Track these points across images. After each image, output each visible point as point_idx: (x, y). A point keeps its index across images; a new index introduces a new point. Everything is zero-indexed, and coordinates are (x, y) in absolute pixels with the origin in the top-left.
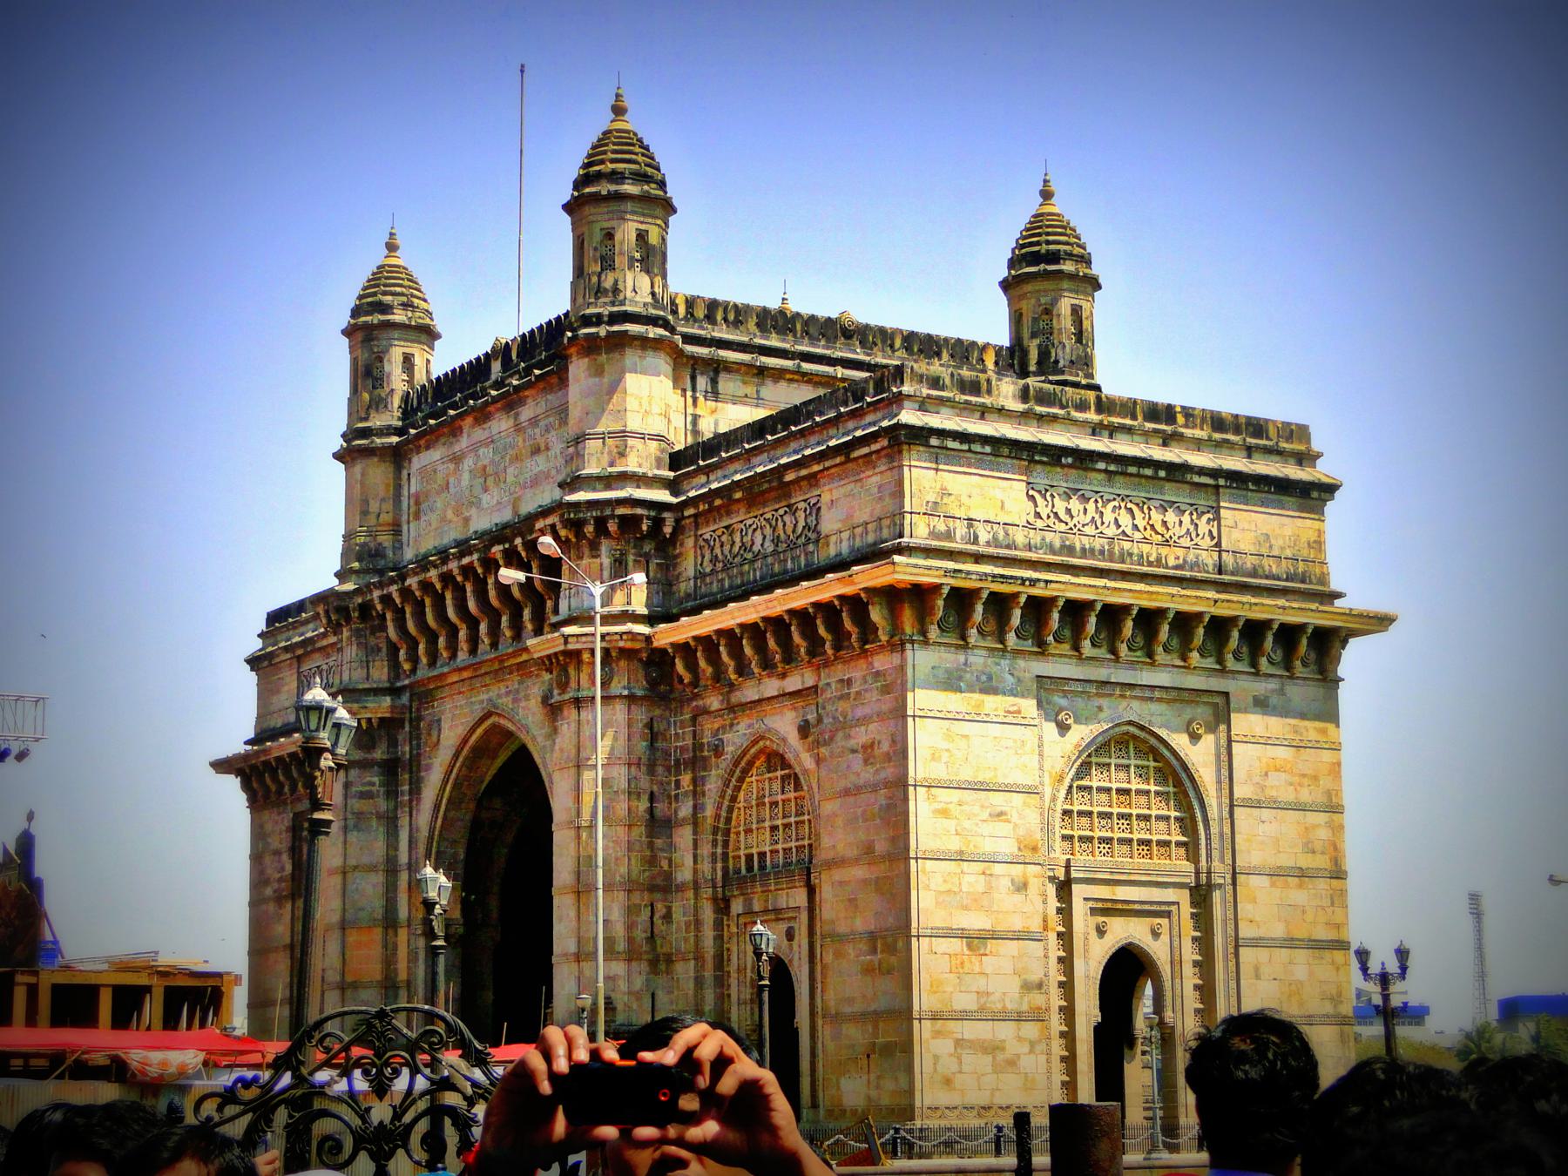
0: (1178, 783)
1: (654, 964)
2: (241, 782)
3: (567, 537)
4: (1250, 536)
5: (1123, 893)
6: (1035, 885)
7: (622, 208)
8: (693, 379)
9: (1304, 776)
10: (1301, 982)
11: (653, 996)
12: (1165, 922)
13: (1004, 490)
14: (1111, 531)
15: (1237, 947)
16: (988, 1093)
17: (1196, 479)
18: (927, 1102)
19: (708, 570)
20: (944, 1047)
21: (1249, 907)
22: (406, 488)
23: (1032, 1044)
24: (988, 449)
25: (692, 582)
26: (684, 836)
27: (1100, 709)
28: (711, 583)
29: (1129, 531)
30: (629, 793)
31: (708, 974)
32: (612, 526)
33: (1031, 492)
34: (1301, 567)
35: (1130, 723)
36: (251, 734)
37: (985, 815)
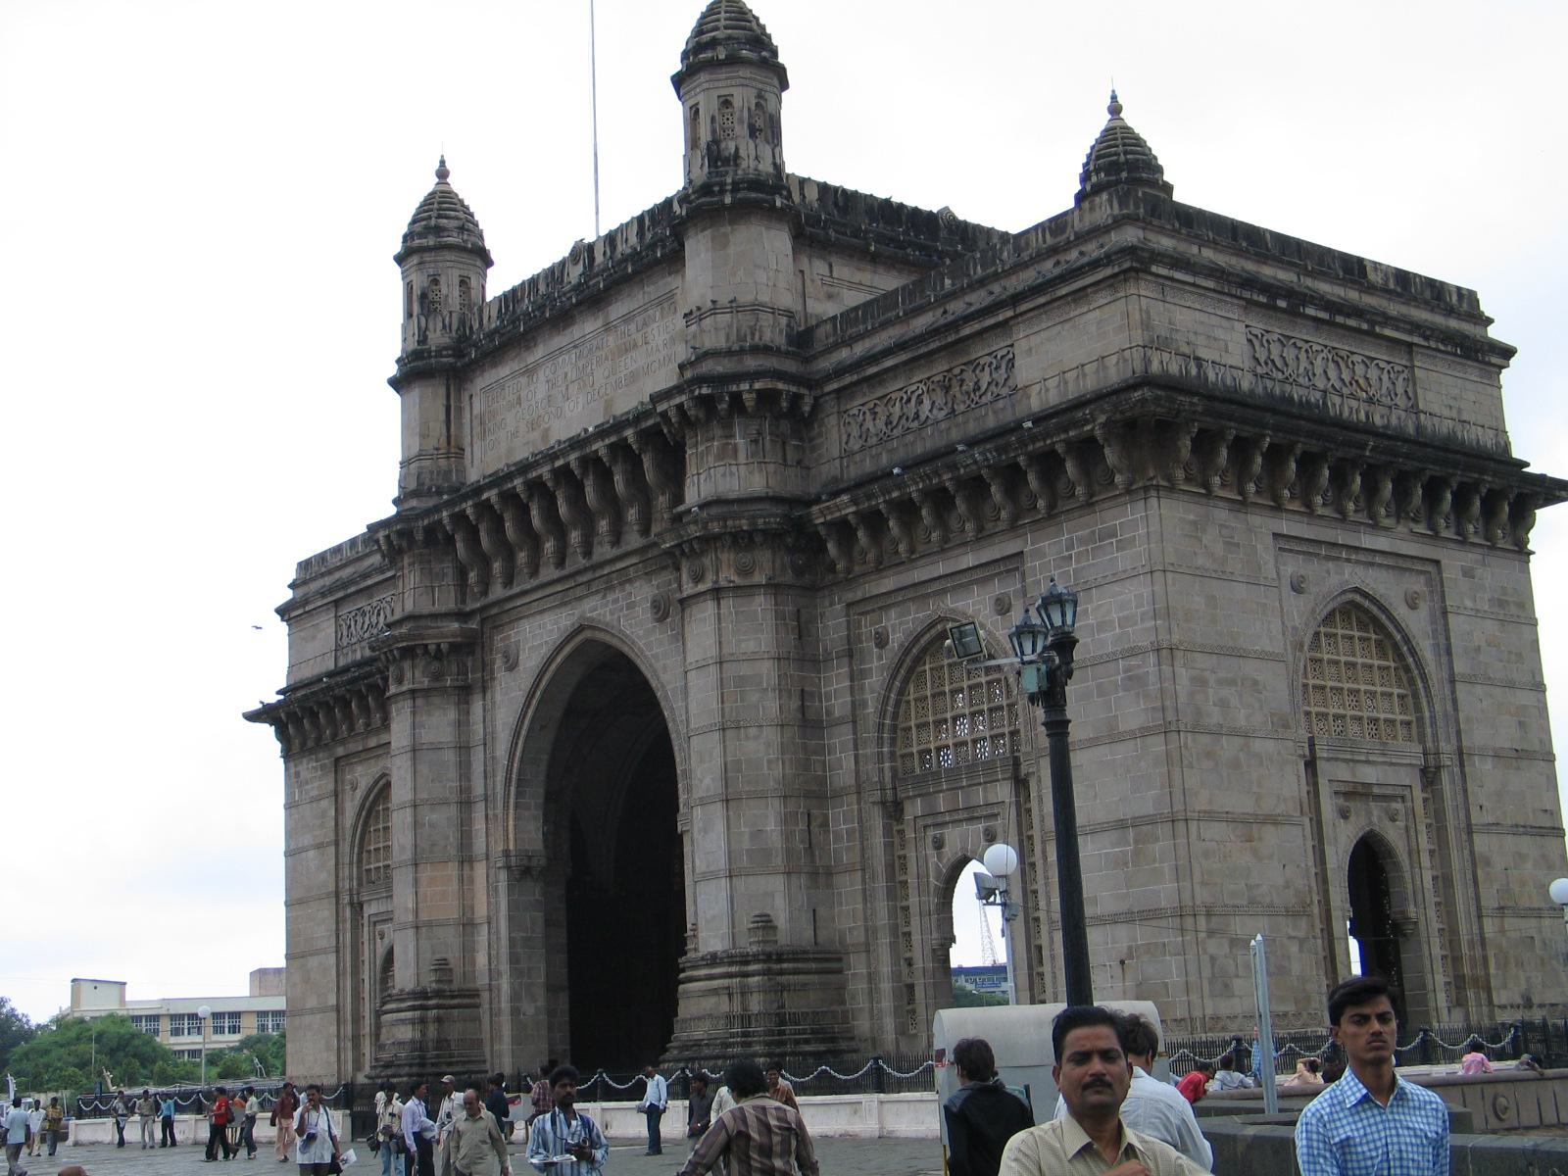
0: (1400, 657)
1: (814, 875)
2: (276, 731)
3: (697, 417)
5: (1369, 775)
7: (741, 74)
14: (1320, 383)
19: (857, 447)
22: (468, 409)
23: (1302, 942)
25: (837, 462)
26: (841, 737)
28: (863, 461)
29: (1338, 385)
30: (780, 691)
31: (881, 884)
32: (749, 399)
33: (1250, 336)
35: (1356, 590)
36: (283, 684)
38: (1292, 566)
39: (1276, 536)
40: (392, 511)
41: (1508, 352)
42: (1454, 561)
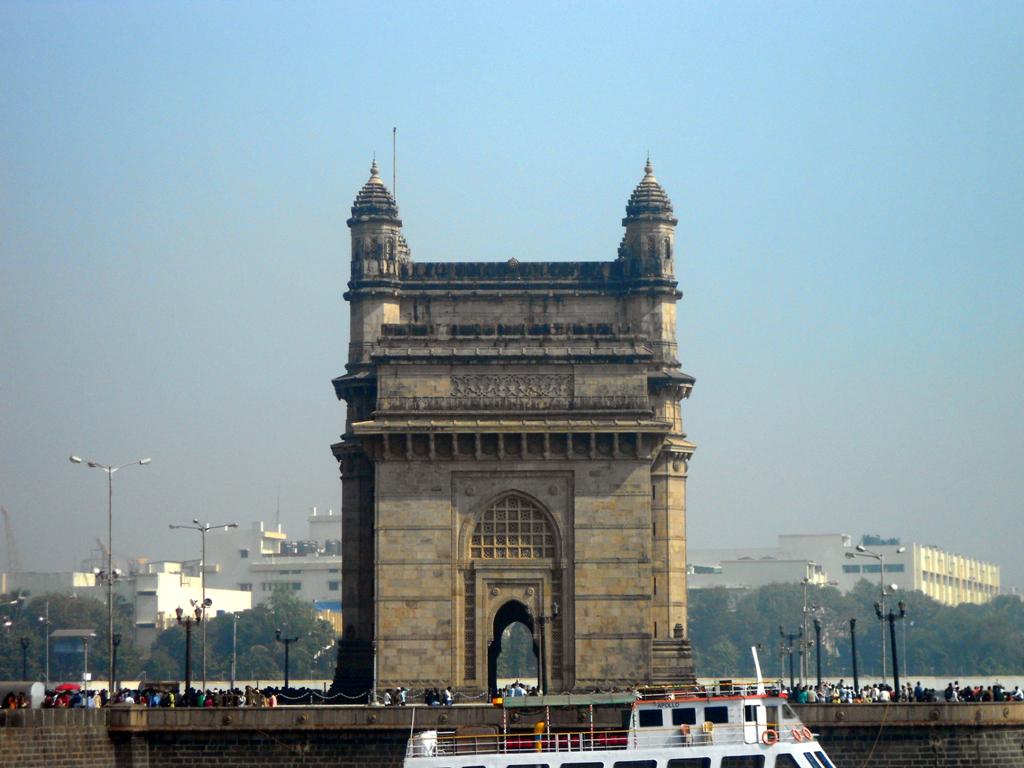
4: (594, 387)
5: (506, 575)
6: (447, 573)
8: (415, 308)
10: (616, 618)
15: (574, 600)
16: (415, 675)
17: (556, 362)
18: (381, 677)
20: (395, 652)
21: (582, 580)
23: (443, 651)
24: (424, 362)
27: (494, 484)
35: (513, 490)
37: (419, 541)
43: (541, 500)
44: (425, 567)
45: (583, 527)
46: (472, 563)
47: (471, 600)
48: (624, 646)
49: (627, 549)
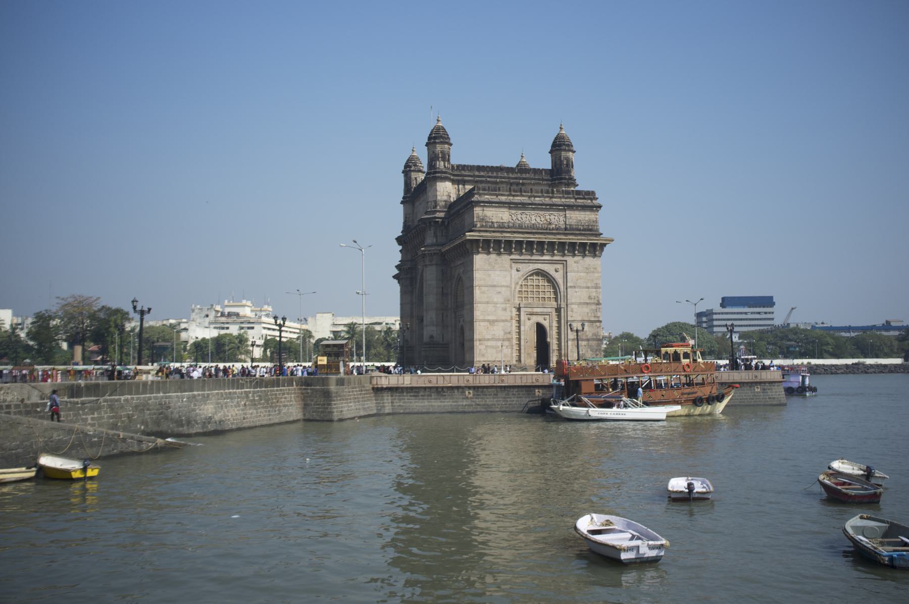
5: (535, 310)
9: (589, 280)
11: (443, 335)
12: (548, 317)
13: (502, 214)
16: (494, 358)
18: (478, 360)
20: (484, 347)
23: (507, 347)
24: (497, 205)
27: (529, 266)
32: (432, 223)
34: (590, 227)
35: (538, 269)
37: (495, 293)
38: (515, 266)
39: (511, 259)
40: (401, 234)
41: (600, 207)
42: (570, 260)
43: (551, 274)
44: (498, 305)
45: (571, 287)
46: (519, 304)
47: (519, 321)
48: (590, 344)
49: (591, 299)
